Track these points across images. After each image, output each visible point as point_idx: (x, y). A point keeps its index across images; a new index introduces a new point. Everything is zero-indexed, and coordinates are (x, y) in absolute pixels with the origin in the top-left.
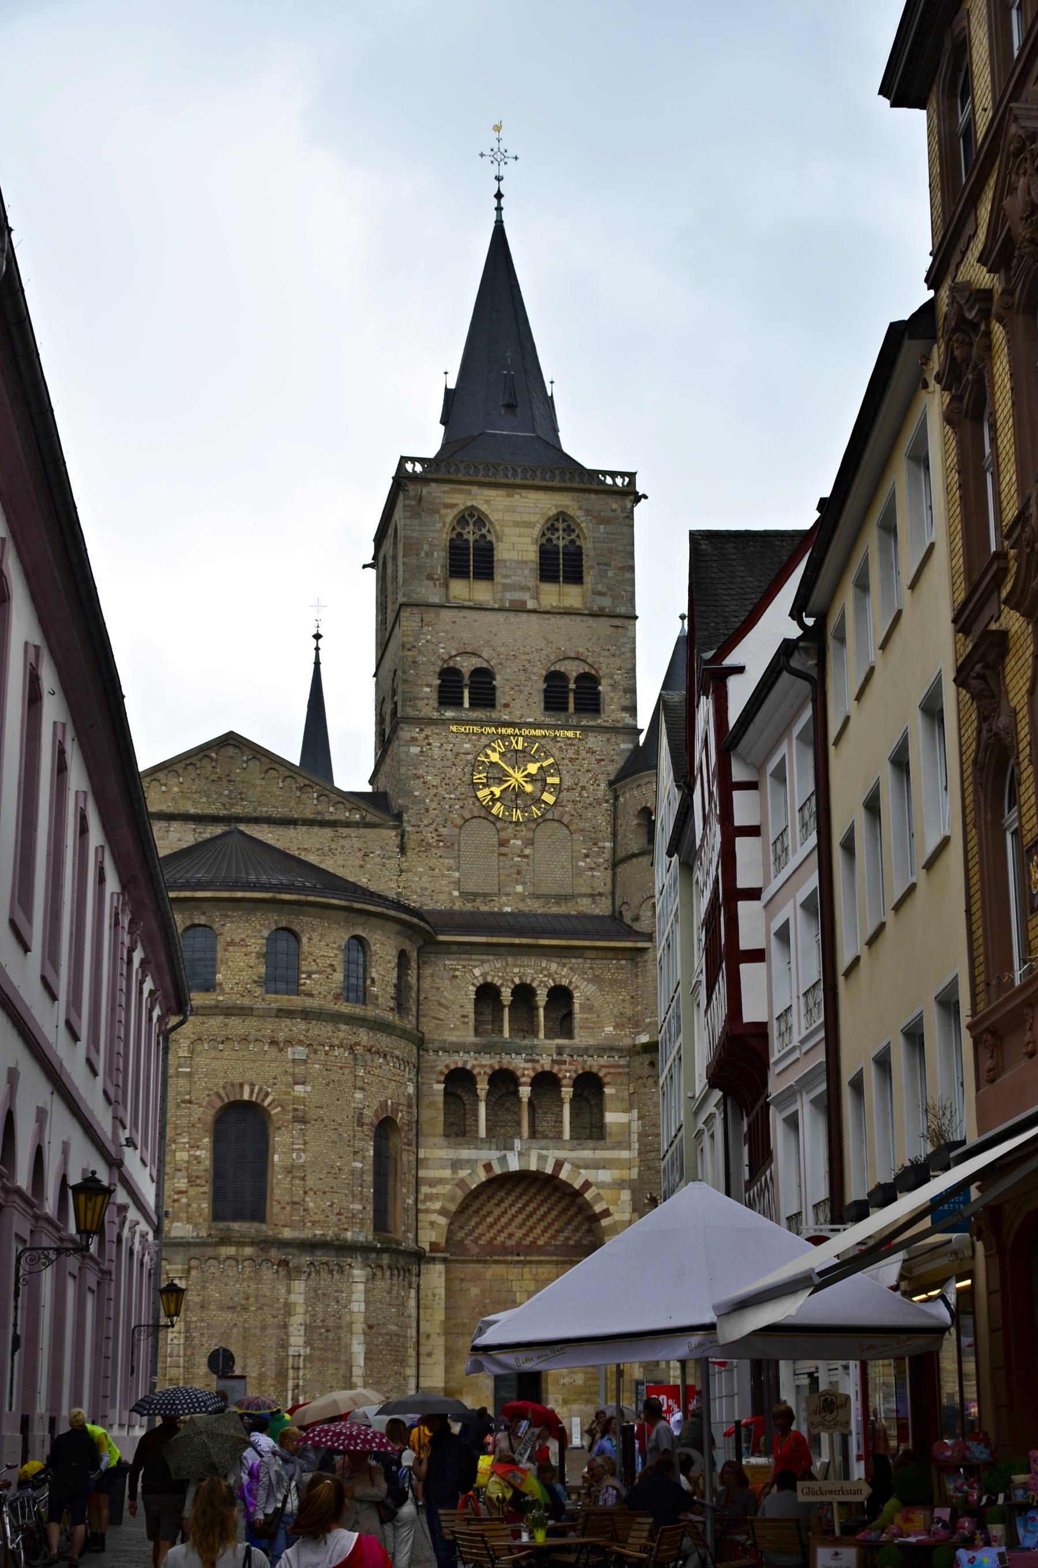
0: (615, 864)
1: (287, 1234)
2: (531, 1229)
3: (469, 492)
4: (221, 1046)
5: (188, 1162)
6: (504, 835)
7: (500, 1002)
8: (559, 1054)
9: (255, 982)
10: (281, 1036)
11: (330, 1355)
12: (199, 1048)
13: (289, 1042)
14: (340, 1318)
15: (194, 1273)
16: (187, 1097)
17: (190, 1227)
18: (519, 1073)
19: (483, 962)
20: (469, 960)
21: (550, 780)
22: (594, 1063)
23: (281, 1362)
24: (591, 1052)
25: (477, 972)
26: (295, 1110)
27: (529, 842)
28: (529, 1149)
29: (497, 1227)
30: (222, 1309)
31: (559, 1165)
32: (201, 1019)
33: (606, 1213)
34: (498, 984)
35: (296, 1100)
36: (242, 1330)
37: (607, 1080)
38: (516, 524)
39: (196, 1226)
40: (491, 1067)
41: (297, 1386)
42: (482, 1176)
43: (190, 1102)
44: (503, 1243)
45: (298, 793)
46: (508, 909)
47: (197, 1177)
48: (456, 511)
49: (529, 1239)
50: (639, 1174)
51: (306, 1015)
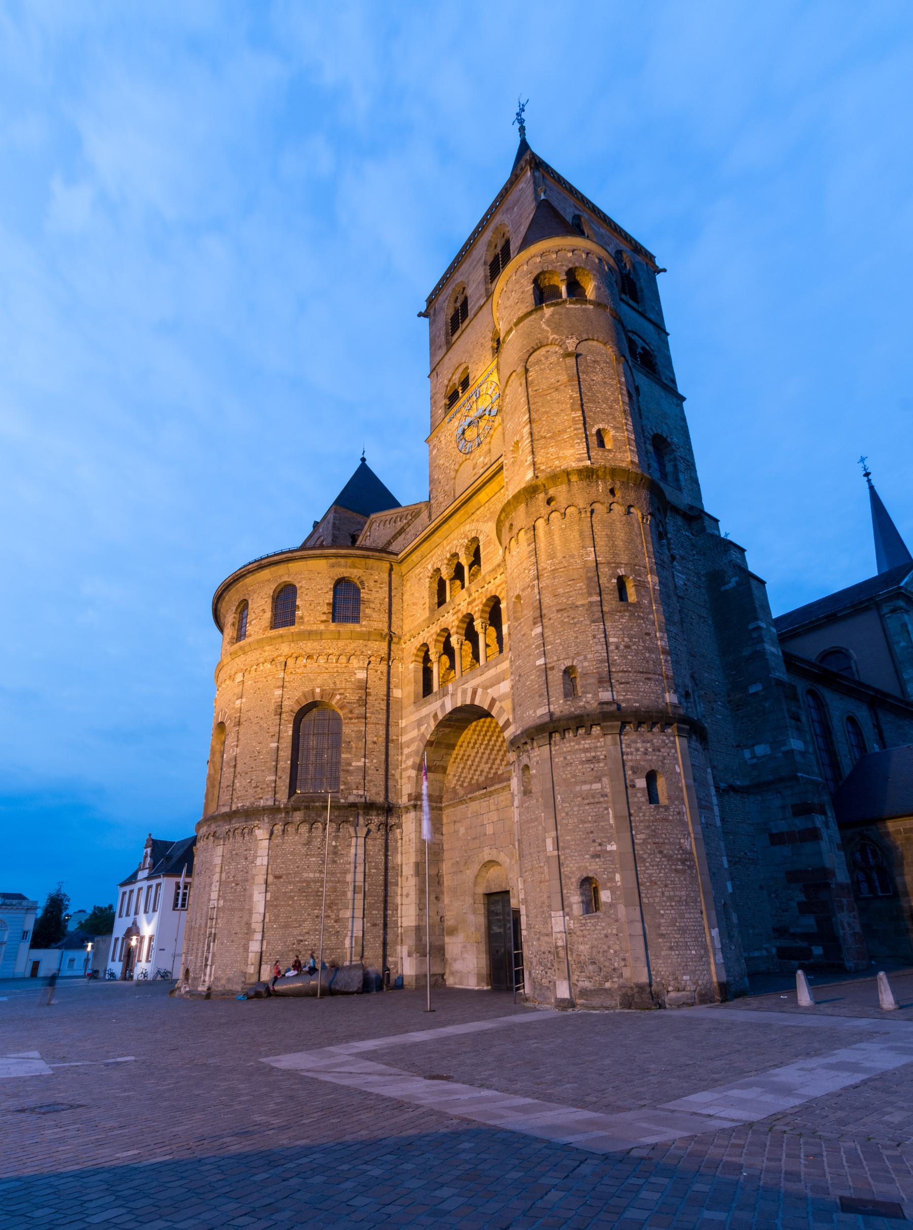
11: (237, 905)
14: (247, 873)
19: (432, 557)
22: (492, 588)
24: (488, 579)
25: (429, 567)
28: (456, 689)
42: (433, 725)
44: (477, 780)
49: (493, 771)
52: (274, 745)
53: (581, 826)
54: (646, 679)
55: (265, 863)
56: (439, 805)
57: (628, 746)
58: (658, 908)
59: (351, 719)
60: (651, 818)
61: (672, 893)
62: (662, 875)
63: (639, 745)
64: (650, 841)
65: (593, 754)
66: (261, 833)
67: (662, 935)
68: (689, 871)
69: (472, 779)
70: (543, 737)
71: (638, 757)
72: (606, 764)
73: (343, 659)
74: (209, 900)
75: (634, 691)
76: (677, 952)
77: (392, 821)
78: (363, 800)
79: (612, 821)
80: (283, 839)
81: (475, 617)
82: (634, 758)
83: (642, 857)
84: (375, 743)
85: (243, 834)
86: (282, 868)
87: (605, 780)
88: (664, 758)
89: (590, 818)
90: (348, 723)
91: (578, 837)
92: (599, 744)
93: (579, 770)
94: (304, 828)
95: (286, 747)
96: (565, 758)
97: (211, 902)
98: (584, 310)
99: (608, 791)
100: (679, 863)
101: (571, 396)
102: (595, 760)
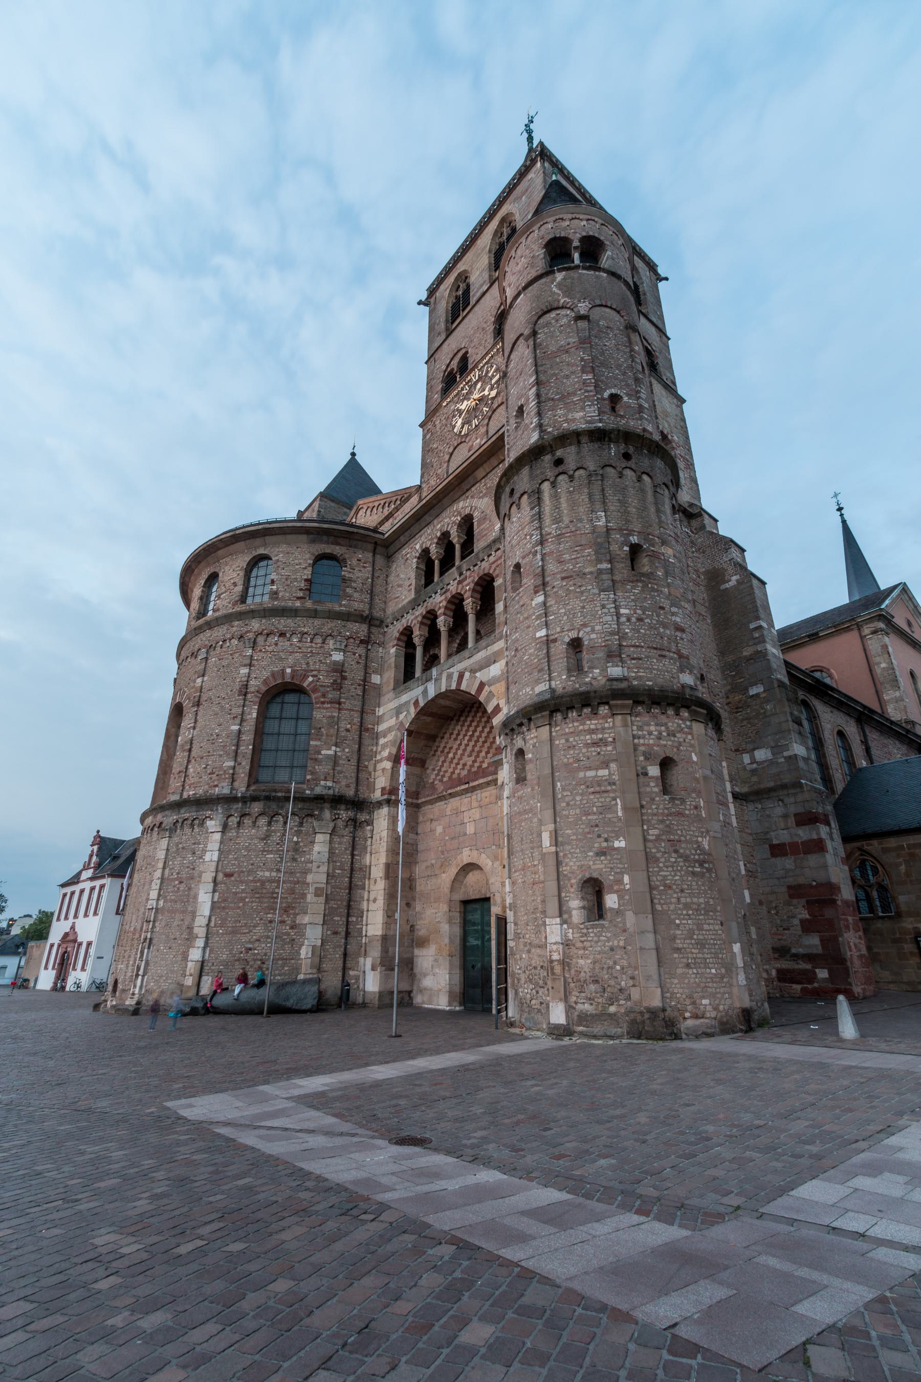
11: (178, 906)
14: (194, 869)
19: (421, 536)
24: (481, 556)
25: (418, 547)
28: (441, 674)
42: (413, 712)
44: (459, 774)
49: (477, 765)
52: (236, 728)
53: (584, 818)
54: (660, 656)
55: (215, 858)
56: (415, 801)
57: (640, 728)
58: (673, 917)
59: (323, 703)
60: (666, 811)
61: (689, 900)
62: (677, 878)
63: (652, 728)
64: (664, 837)
65: (600, 736)
66: (213, 825)
67: (678, 950)
68: (707, 875)
69: (453, 773)
70: (543, 716)
71: (651, 742)
72: (615, 748)
73: (319, 640)
74: (148, 899)
75: (647, 668)
76: (695, 971)
77: (363, 817)
78: (331, 792)
79: (620, 814)
80: (238, 833)
81: (465, 596)
82: (646, 741)
83: (655, 857)
84: (348, 730)
85: (192, 826)
86: (234, 864)
87: (613, 766)
88: (680, 744)
89: (595, 809)
90: (319, 708)
91: (581, 830)
92: (607, 725)
93: (584, 754)
94: (263, 821)
95: (249, 731)
96: (567, 740)
97: (150, 902)
98: (597, 277)
99: (617, 778)
100: (697, 865)
101: (582, 359)
102: (601, 742)
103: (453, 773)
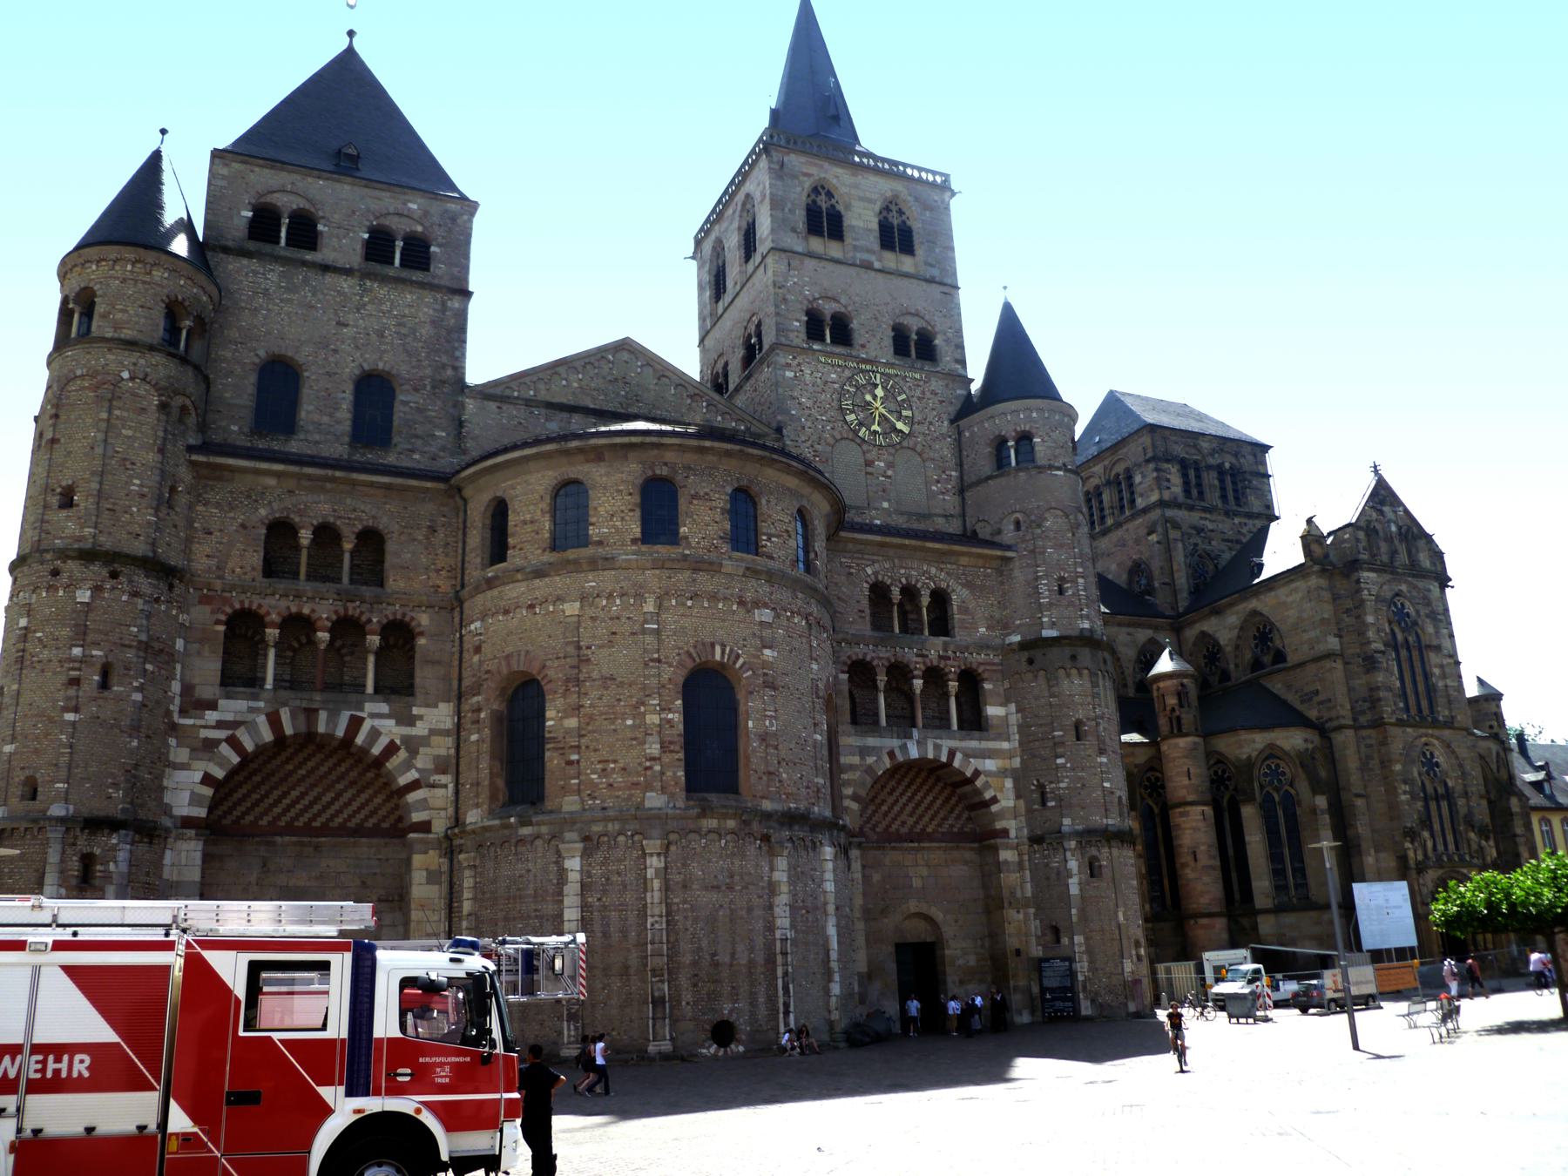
0: (962, 490)
1: (767, 805)
2: (921, 817)
3: (822, 167)
4: (689, 603)
5: (660, 725)
6: (870, 457)
7: (890, 599)
8: (945, 650)
9: (721, 538)
10: (749, 596)
12: (666, 604)
13: (757, 604)
15: (673, 848)
16: (656, 656)
17: (664, 798)
18: (912, 666)
20: (863, 559)
21: (905, 413)
22: (976, 659)
23: (770, 946)
24: (971, 650)
25: (869, 571)
26: (765, 674)
27: (890, 465)
28: (925, 738)
29: (891, 815)
30: (706, 888)
31: (952, 754)
32: (667, 573)
33: (994, 800)
34: (889, 582)
35: (765, 664)
36: (728, 912)
37: (985, 675)
38: (861, 199)
39: (672, 796)
40: (888, 659)
41: (786, 974)
42: (887, 763)
43: (659, 661)
44: (897, 830)
45: (689, 401)
46: (878, 522)
47: (671, 743)
48: (812, 179)
49: (920, 827)
50: (1021, 763)
51: (771, 577)
103: (889, 826)
